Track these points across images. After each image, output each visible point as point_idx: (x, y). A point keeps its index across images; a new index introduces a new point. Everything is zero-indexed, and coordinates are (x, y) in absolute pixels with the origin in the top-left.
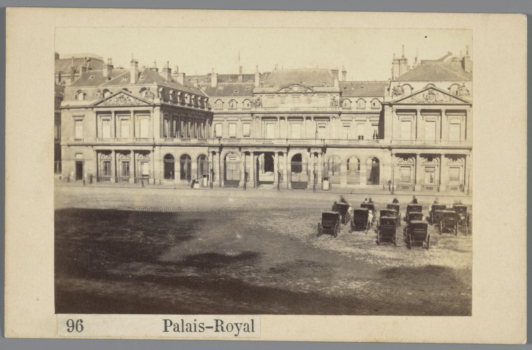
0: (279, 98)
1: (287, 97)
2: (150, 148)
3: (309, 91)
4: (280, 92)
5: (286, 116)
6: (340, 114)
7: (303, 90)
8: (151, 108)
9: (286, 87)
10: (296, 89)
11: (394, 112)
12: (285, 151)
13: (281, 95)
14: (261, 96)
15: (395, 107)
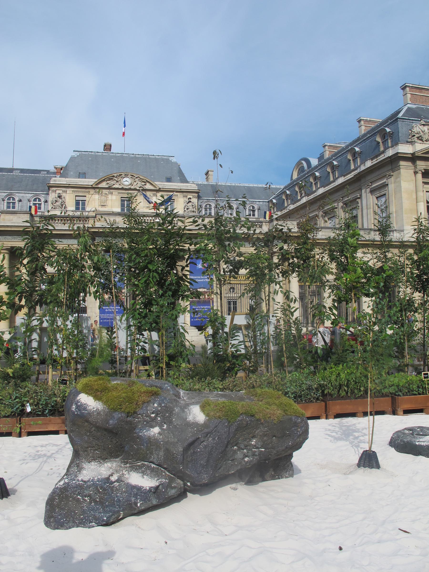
1: (110, 196)
3: (148, 186)
9: (110, 179)
10: (127, 182)
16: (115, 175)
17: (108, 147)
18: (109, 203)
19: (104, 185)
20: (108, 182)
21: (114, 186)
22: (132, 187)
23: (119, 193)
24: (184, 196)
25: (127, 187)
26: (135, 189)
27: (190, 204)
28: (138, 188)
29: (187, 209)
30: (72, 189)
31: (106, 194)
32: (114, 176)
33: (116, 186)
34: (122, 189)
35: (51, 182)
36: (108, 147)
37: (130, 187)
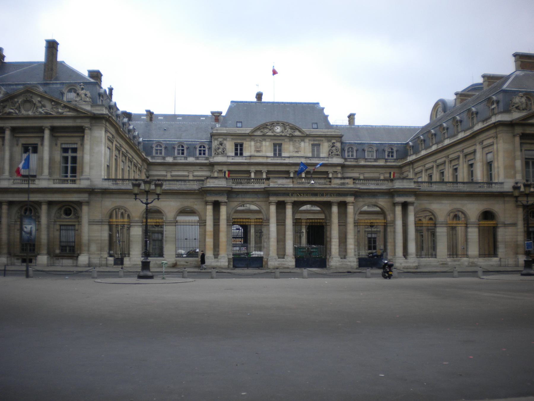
0: (253, 143)
1: (264, 143)
2: (83, 197)
3: (297, 133)
4: (255, 134)
5: (264, 169)
6: (343, 166)
7: (289, 131)
8: (85, 123)
9: (264, 128)
10: (278, 129)
11: (517, 139)
12: (350, 199)
13: (256, 138)
14: (225, 139)
15: (519, 130)
16: (268, 124)
17: (259, 96)
18: (264, 148)
19: (259, 133)
20: (262, 130)
21: (268, 134)
22: (283, 134)
23: (271, 140)
24: (329, 141)
25: (279, 134)
26: (286, 136)
27: (334, 148)
28: (288, 135)
29: (332, 153)
30: (232, 137)
31: (260, 140)
32: (267, 125)
33: (270, 133)
34: (275, 136)
35: (214, 132)
36: (259, 96)
37: (281, 134)
